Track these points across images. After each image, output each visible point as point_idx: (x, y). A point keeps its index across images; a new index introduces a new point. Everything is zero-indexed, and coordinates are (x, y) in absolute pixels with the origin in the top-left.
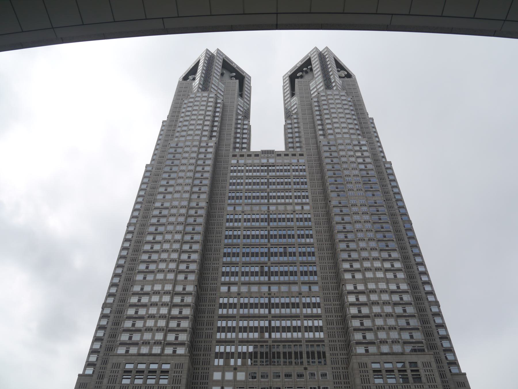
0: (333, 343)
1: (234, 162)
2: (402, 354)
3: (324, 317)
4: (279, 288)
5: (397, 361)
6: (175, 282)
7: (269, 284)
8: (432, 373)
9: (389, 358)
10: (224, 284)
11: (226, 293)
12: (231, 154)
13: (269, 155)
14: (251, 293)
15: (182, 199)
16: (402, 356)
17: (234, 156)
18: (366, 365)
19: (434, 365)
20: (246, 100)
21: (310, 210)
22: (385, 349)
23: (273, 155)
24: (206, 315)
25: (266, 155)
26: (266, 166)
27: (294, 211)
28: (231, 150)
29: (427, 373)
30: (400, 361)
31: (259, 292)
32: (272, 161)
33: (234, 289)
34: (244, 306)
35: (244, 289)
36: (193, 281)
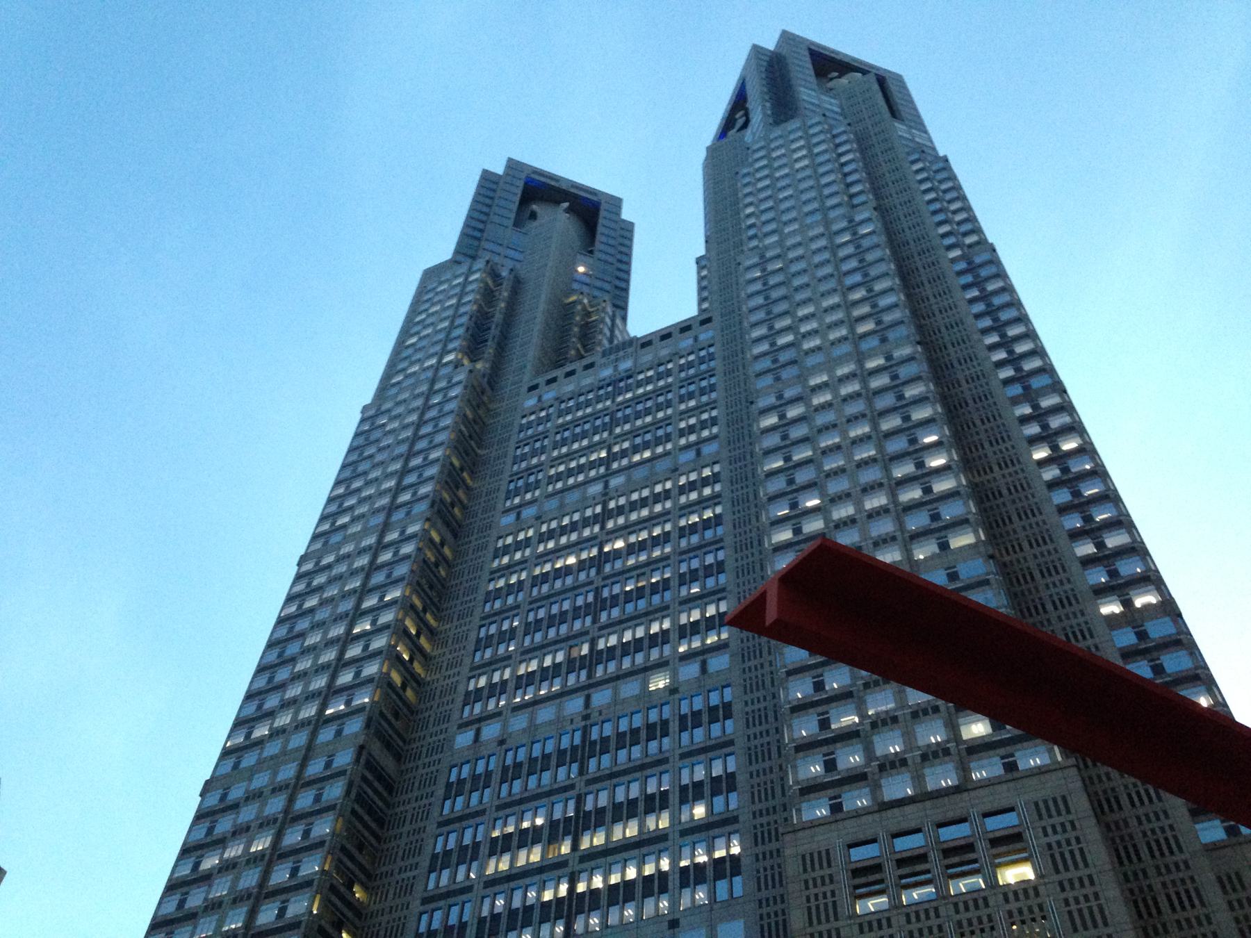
0: (764, 820)
1: (531, 402)
2: (956, 790)
3: (740, 743)
4: (616, 693)
5: (940, 818)
6: (308, 753)
8: (1071, 835)
9: (911, 816)
10: (464, 726)
11: (469, 748)
12: (525, 389)
13: (621, 353)
14: (536, 727)
15: (365, 532)
16: (957, 797)
17: (533, 388)
18: (826, 858)
19: (1080, 804)
20: (603, 257)
21: (718, 453)
22: (899, 787)
23: (630, 350)
24: (407, 828)
25: (613, 357)
26: (609, 385)
27: (676, 470)
28: (526, 378)
29: (1053, 839)
30: (951, 815)
31: (559, 720)
33: (491, 731)
34: (511, 773)
35: (519, 723)
36: (356, 735)
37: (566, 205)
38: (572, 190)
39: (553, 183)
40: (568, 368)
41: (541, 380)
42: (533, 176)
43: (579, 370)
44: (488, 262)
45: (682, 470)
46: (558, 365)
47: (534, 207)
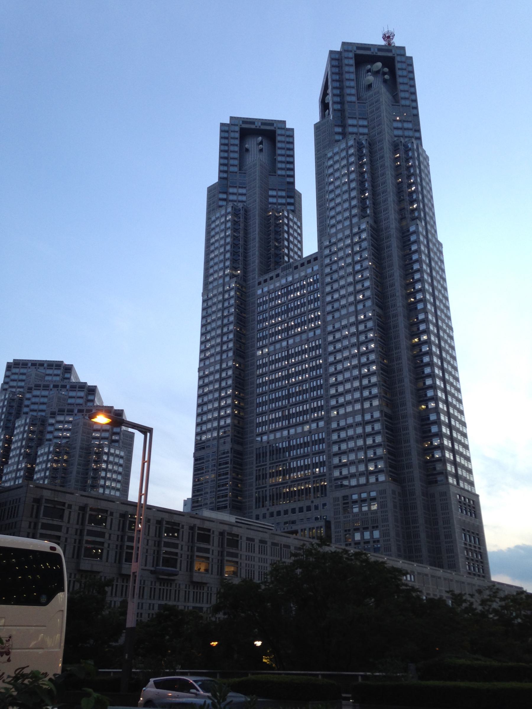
7: (288, 427)
12: (257, 283)
17: (259, 283)
23: (291, 270)
25: (285, 272)
28: (257, 277)
32: (290, 279)
37: (260, 138)
38: (263, 127)
39: (253, 127)
40: (271, 275)
41: (262, 279)
42: (245, 126)
43: (274, 277)
44: (232, 207)
45: (310, 340)
46: (267, 271)
47: (247, 146)
